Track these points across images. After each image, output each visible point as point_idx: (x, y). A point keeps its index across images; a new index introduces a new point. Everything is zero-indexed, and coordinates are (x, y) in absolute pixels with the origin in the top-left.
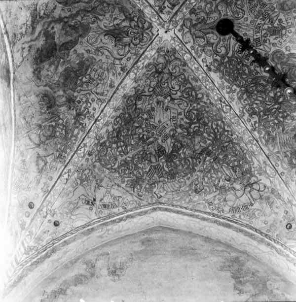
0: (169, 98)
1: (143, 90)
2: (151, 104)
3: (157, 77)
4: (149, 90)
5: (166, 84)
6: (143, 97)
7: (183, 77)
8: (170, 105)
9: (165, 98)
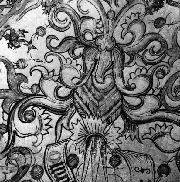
0: (120, 122)
1: (39, 86)
2: (67, 140)
3: (81, 55)
4: (57, 89)
5: (108, 80)
6: (39, 111)
7: (156, 45)
8: (127, 144)
9: (109, 122)
